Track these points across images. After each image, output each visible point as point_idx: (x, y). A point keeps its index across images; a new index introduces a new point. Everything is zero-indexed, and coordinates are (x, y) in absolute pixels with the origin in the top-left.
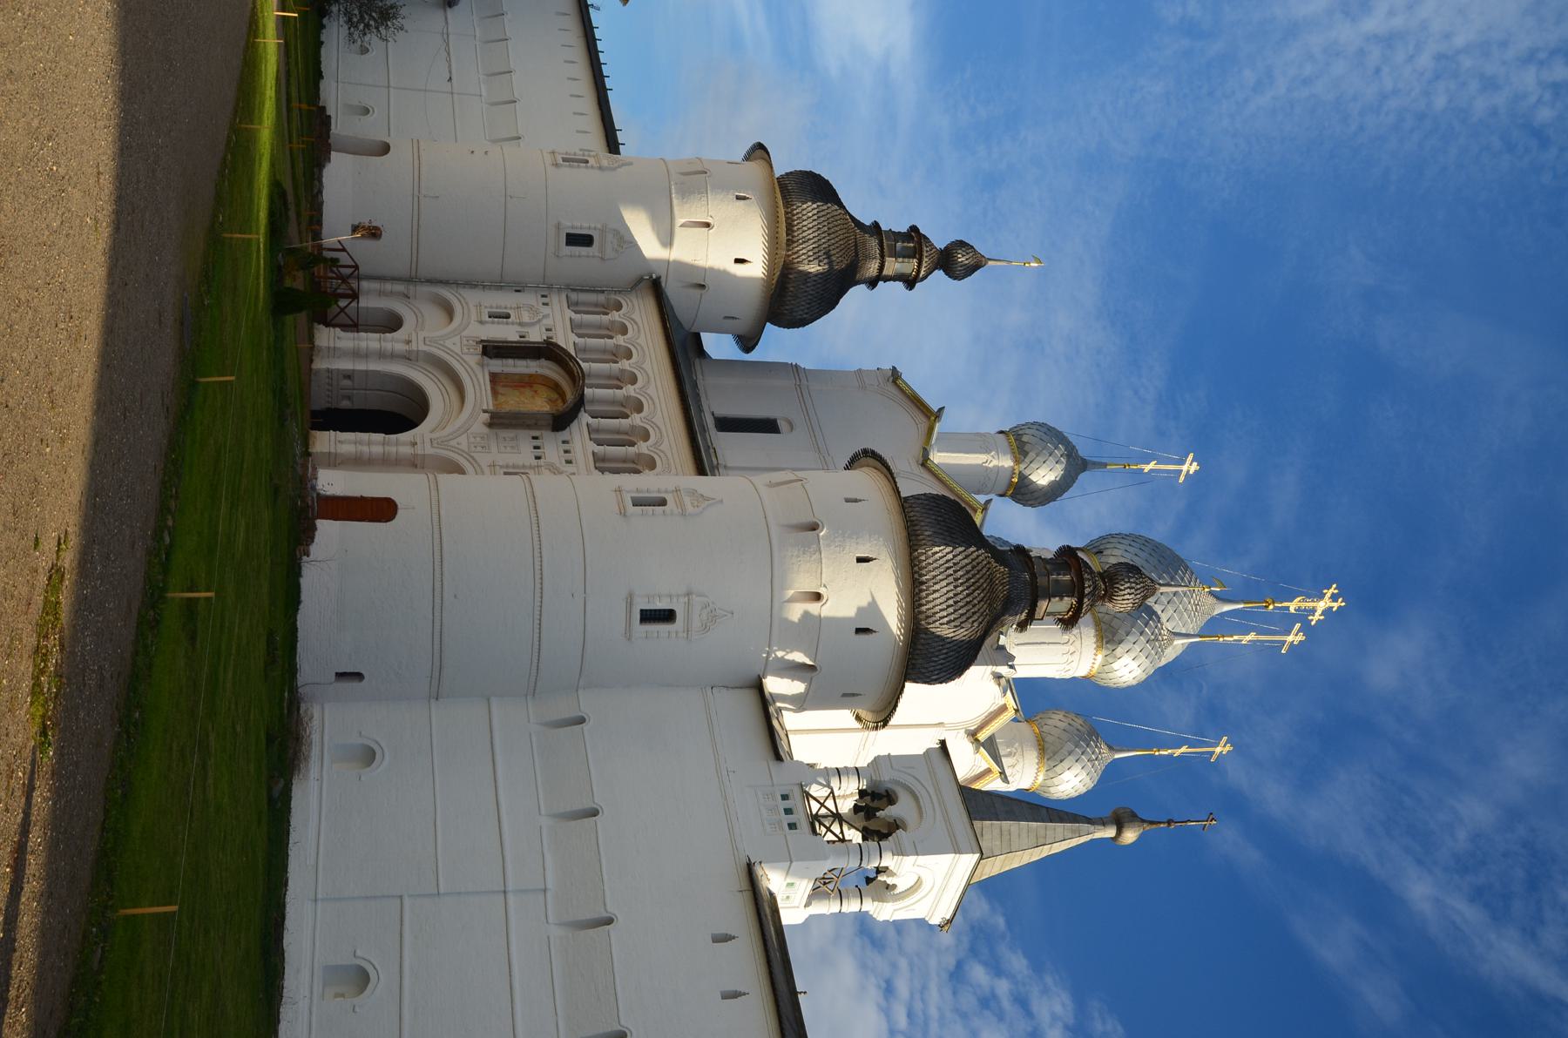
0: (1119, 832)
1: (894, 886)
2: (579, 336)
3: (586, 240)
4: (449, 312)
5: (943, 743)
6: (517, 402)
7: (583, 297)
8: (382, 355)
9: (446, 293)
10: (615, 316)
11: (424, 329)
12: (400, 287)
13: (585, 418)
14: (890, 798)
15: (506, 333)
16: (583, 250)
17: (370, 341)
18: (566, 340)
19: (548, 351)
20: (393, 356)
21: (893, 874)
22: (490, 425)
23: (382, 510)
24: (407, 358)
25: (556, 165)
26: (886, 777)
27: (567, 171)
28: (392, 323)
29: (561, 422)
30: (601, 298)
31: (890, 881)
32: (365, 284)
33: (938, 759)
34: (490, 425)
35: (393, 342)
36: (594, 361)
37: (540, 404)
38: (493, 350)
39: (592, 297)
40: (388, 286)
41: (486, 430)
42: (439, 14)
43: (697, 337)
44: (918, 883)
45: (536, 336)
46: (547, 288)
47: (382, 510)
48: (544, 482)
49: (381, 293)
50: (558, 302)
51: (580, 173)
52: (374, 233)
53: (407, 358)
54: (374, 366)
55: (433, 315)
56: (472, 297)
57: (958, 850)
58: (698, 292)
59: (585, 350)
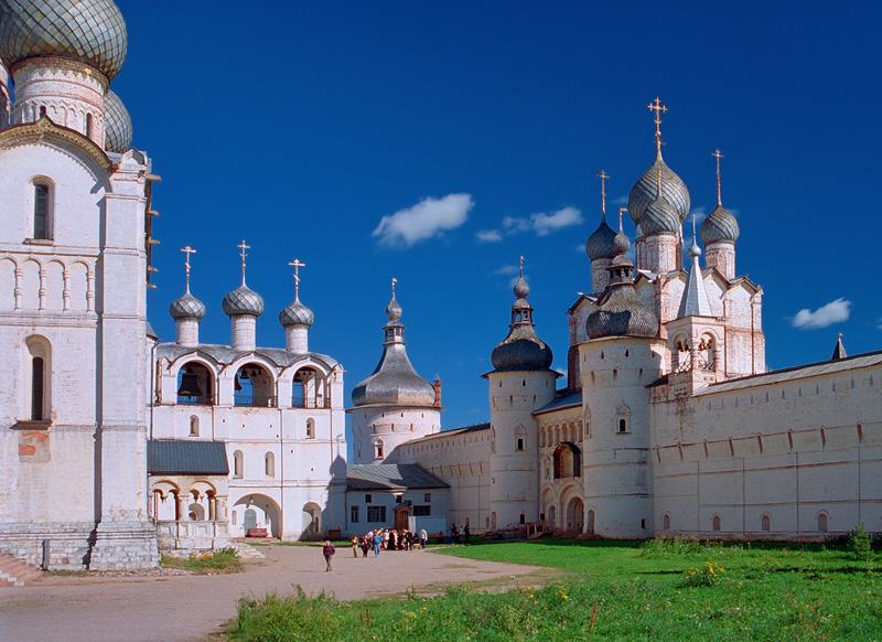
0: (695, 255)
1: (710, 341)
3: (520, 442)
4: (547, 490)
6: (570, 469)
7: (541, 441)
8: (562, 513)
9: (542, 491)
11: (553, 497)
13: (576, 443)
14: (680, 343)
17: (558, 516)
19: (557, 456)
20: (562, 509)
23: (591, 512)
24: (562, 504)
27: (497, 449)
28: (553, 508)
29: (577, 452)
33: (669, 326)
35: (558, 508)
37: (569, 457)
38: (557, 476)
39: (541, 438)
42: (452, 489)
43: (559, 392)
44: (707, 333)
45: (552, 459)
46: (538, 455)
47: (591, 512)
51: (498, 441)
52: (522, 517)
53: (562, 504)
54: (565, 516)
55: (549, 496)
56: (543, 481)
59: (558, 440)
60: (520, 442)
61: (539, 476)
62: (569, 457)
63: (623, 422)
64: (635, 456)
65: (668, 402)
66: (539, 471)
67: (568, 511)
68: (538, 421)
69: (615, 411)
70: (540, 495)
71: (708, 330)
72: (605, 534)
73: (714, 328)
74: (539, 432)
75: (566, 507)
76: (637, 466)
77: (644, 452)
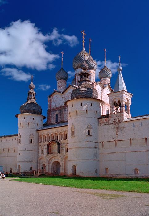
2: (42, 141)
3: (31, 140)
5: (107, 94)
9: (39, 159)
10: (42, 136)
12: (39, 164)
14: (115, 102)
15: (45, 151)
16: (33, 140)
18: (46, 143)
19: (48, 145)
21: (126, 102)
22: (60, 153)
25: (20, 143)
26: (112, 102)
30: (39, 138)
31: (126, 102)
32: (38, 169)
34: (60, 153)
36: (42, 140)
37: (55, 147)
38: (48, 153)
39: (39, 139)
40: (38, 166)
41: (60, 154)
44: (127, 99)
45: (46, 147)
46: (38, 146)
48: (69, 146)
49: (39, 167)
50: (40, 144)
51: (21, 141)
52: (31, 168)
54: (50, 168)
55: (42, 160)
56: (40, 155)
57: (123, 93)
58: (38, 125)
60: (31, 140)
61: (38, 153)
62: (55, 147)
63: (89, 131)
64: (93, 145)
65: (109, 124)
66: (38, 152)
67: (52, 166)
68: (38, 133)
69: (86, 127)
70: (38, 160)
71: (127, 98)
72: (81, 175)
73: (129, 97)
74: (39, 137)
75: (51, 165)
76: (95, 149)
77: (96, 143)
